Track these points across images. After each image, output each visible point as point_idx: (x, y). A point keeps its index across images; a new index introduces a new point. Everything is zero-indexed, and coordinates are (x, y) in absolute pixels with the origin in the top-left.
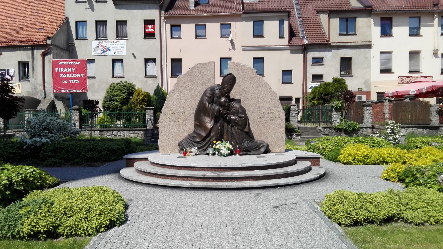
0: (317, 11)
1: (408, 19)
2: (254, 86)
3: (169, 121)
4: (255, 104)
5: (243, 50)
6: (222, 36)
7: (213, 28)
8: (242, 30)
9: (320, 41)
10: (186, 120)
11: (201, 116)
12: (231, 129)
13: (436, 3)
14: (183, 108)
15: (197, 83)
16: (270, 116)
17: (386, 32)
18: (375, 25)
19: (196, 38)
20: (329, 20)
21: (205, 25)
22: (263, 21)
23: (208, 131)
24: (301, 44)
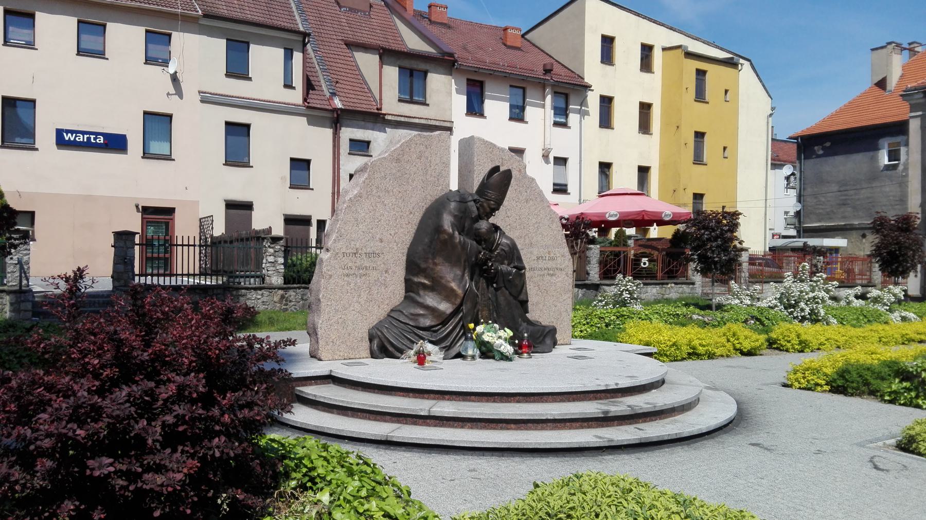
0: (346, 44)
1: (508, 88)
3: (348, 275)
5: (202, 101)
6: (149, 61)
7: (126, 39)
8: (199, 55)
9: (364, 106)
10: (386, 272)
11: (435, 264)
12: (496, 296)
13: (548, 68)
14: (381, 241)
15: (413, 181)
17: (475, 109)
18: (458, 92)
19: (78, 54)
20: (381, 68)
21: (104, 26)
22: (248, 44)
23: (458, 301)
24: (330, 108)
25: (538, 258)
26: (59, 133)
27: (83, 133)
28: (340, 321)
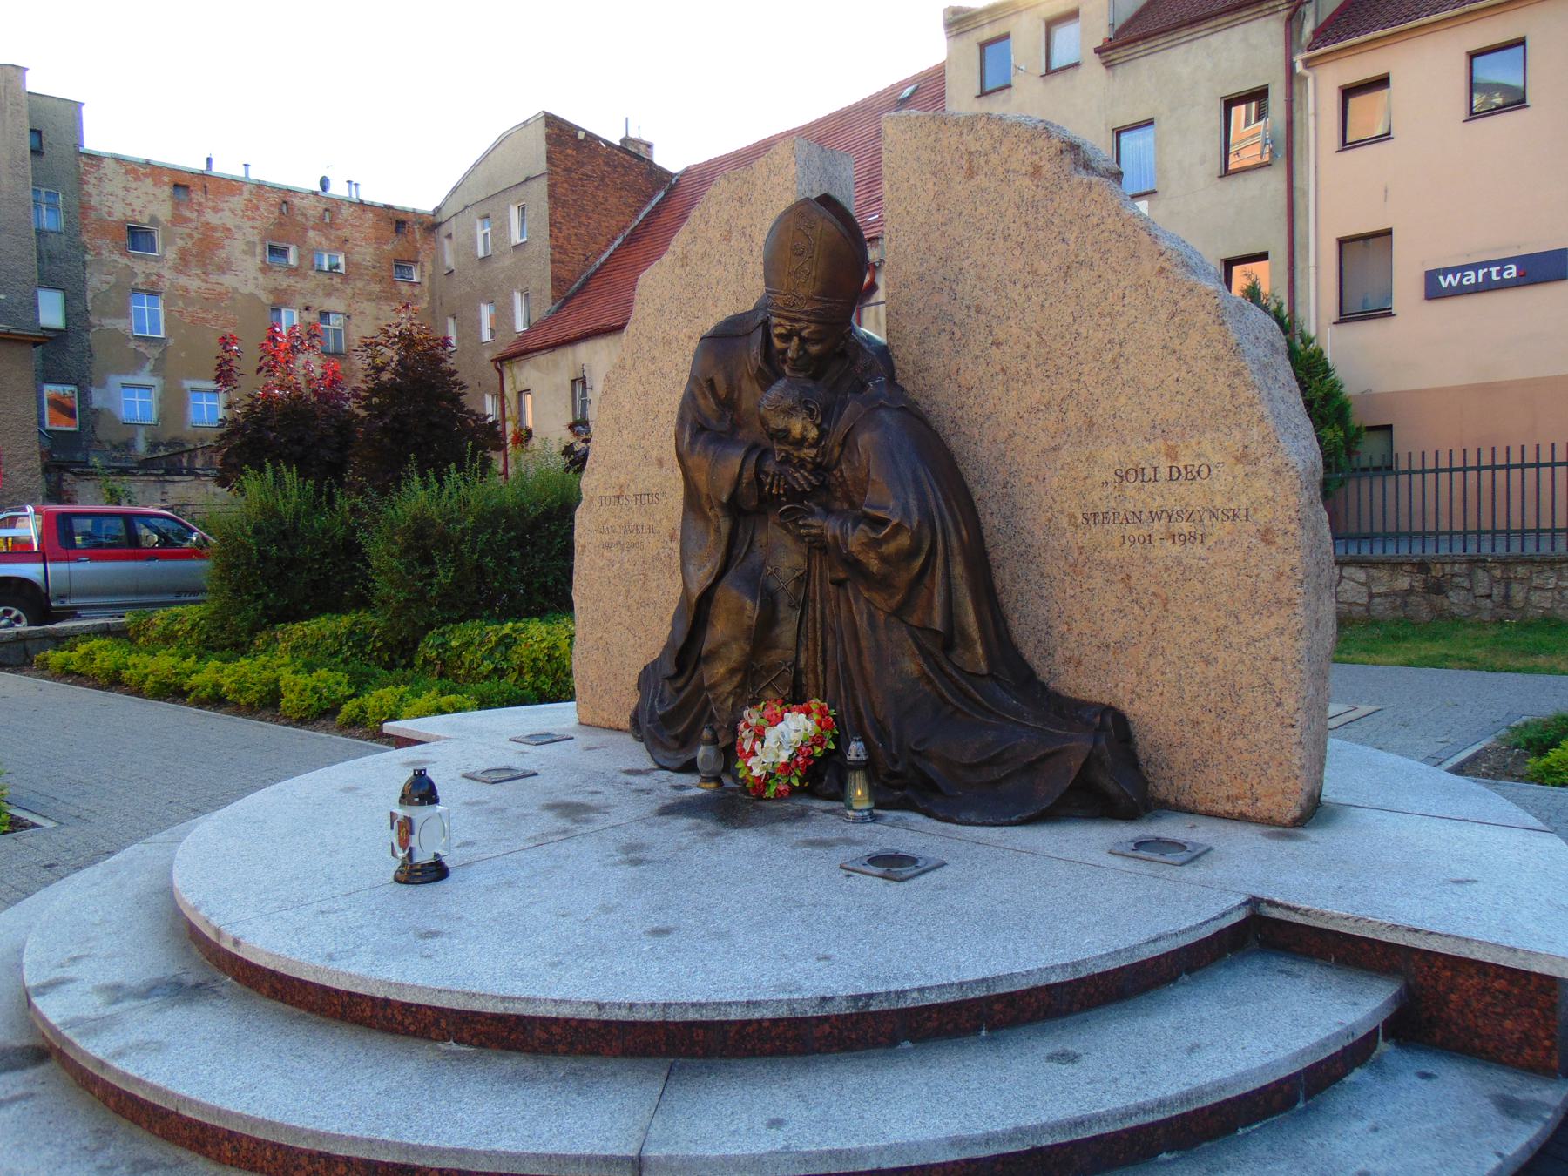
2: (1043, 268)
3: (608, 546)
4: (1054, 414)
16: (1172, 504)
25: (1122, 477)
26: (1431, 277)
27: (1475, 267)
28: (601, 643)
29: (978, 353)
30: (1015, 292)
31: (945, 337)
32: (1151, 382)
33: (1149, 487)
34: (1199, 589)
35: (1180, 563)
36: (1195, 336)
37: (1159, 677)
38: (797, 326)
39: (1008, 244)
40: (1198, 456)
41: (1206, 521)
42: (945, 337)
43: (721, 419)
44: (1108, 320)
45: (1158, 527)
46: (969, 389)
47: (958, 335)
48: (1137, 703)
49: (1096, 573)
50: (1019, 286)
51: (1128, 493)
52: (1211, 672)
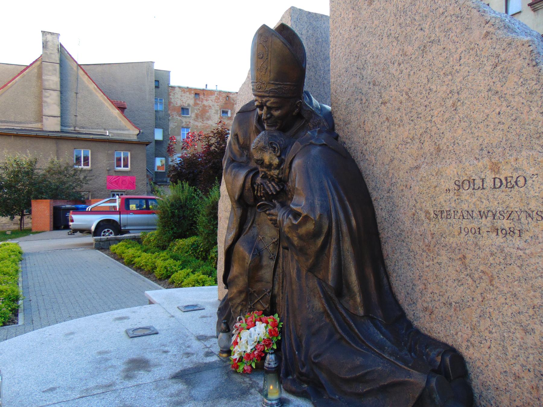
2: (409, 49)
4: (417, 144)
16: (494, 206)
25: (460, 186)
29: (374, 110)
30: (393, 69)
31: (358, 102)
32: (479, 117)
33: (478, 193)
34: (518, 272)
35: (502, 251)
36: (513, 78)
37: (487, 334)
38: (264, 100)
39: (390, 40)
40: (516, 169)
41: (523, 220)
42: (358, 102)
43: (242, 155)
44: (450, 77)
45: (486, 222)
46: (370, 132)
47: (364, 101)
48: (471, 350)
49: (443, 252)
50: (396, 64)
51: (463, 197)
52: (530, 340)
